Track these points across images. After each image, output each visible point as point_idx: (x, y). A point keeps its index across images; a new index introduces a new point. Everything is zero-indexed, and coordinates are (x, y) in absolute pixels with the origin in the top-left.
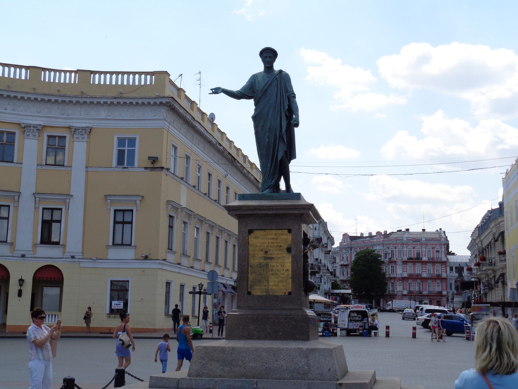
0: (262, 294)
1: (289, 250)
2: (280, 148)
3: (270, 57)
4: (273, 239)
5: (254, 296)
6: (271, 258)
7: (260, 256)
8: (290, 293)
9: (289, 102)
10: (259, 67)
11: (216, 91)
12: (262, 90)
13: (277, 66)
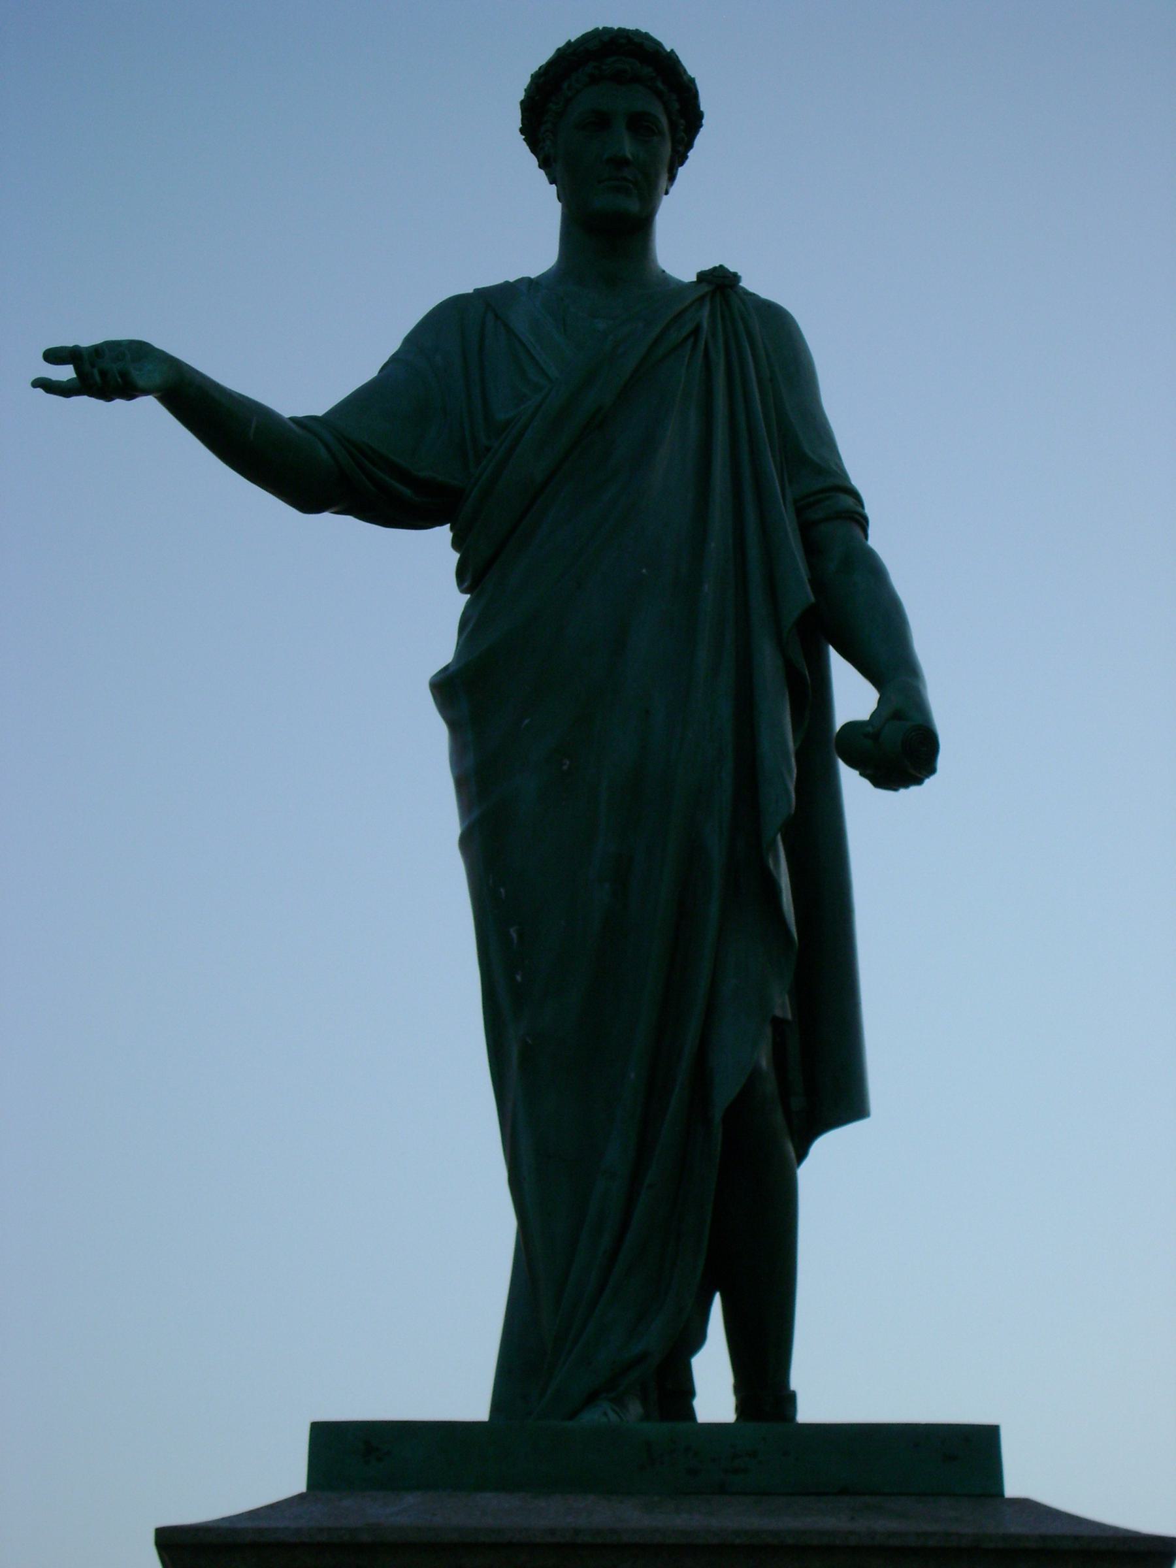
3: (640, 125)
9: (812, 567)
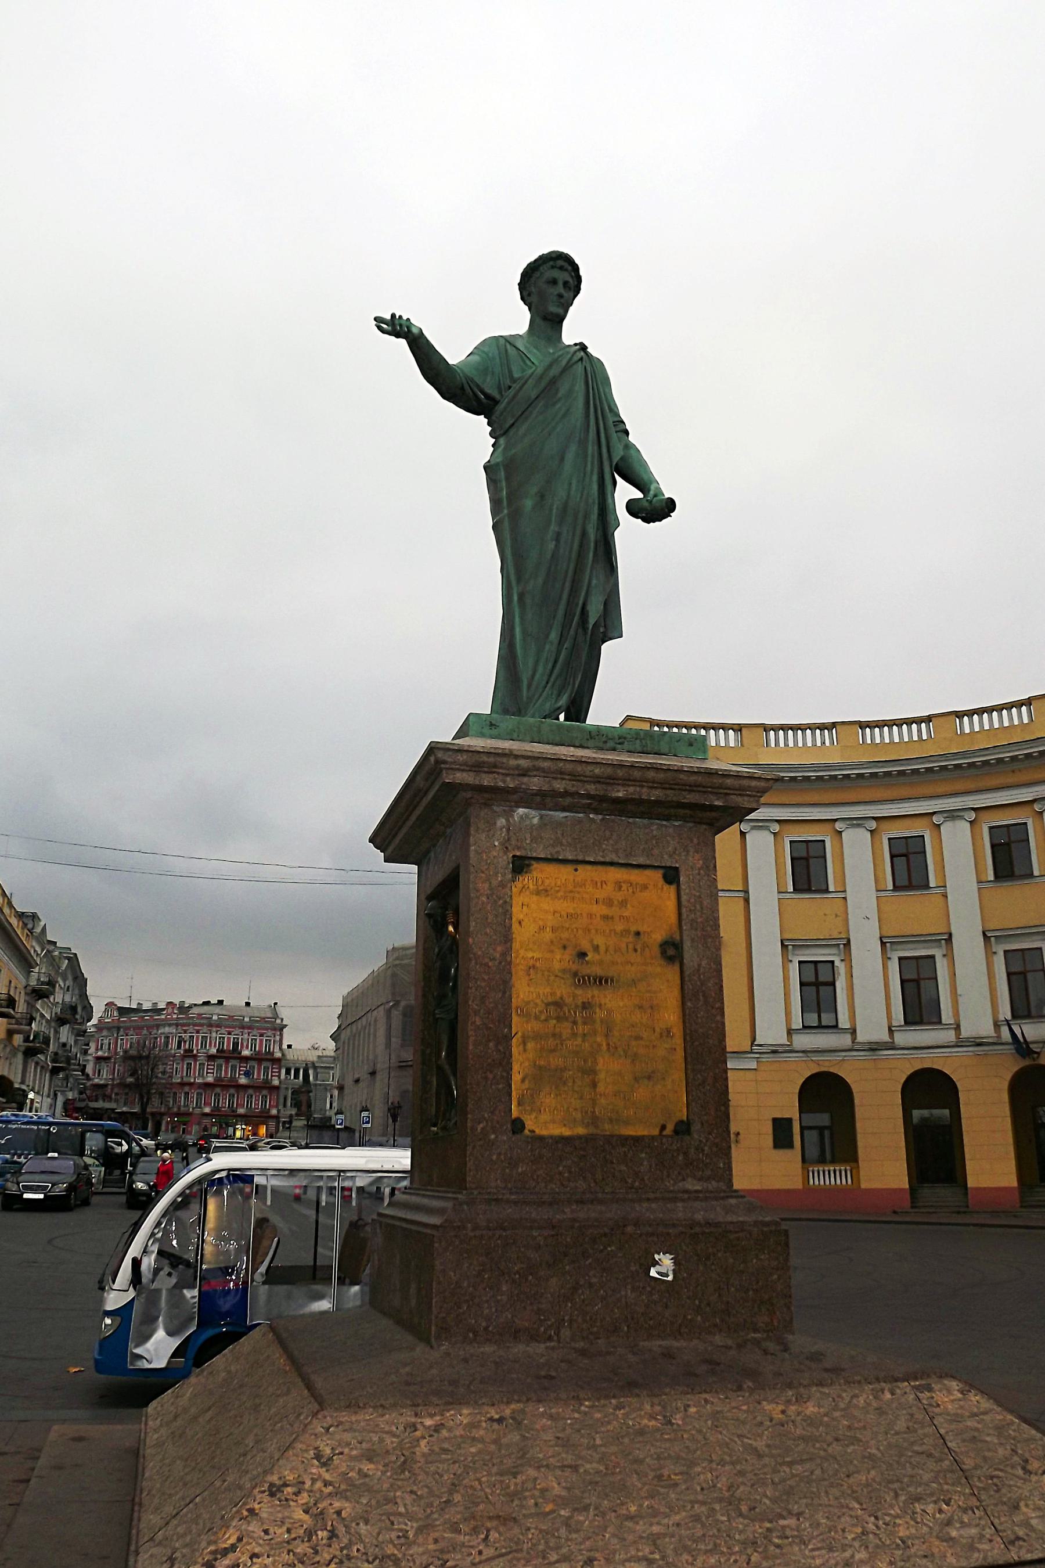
0: (567, 1132)
1: (671, 950)
2: (594, 582)
4: (609, 902)
5: (541, 1138)
6: (601, 981)
7: (557, 966)
8: (683, 1129)
10: (516, 319)
11: (395, 327)
12: (541, 377)
13: (571, 333)
